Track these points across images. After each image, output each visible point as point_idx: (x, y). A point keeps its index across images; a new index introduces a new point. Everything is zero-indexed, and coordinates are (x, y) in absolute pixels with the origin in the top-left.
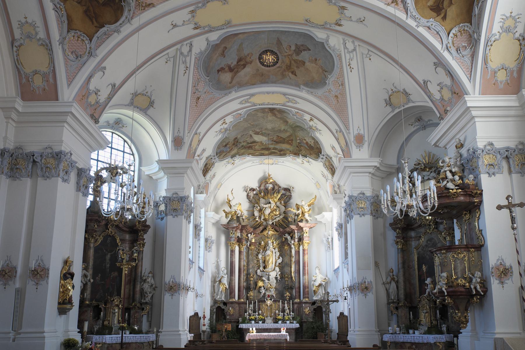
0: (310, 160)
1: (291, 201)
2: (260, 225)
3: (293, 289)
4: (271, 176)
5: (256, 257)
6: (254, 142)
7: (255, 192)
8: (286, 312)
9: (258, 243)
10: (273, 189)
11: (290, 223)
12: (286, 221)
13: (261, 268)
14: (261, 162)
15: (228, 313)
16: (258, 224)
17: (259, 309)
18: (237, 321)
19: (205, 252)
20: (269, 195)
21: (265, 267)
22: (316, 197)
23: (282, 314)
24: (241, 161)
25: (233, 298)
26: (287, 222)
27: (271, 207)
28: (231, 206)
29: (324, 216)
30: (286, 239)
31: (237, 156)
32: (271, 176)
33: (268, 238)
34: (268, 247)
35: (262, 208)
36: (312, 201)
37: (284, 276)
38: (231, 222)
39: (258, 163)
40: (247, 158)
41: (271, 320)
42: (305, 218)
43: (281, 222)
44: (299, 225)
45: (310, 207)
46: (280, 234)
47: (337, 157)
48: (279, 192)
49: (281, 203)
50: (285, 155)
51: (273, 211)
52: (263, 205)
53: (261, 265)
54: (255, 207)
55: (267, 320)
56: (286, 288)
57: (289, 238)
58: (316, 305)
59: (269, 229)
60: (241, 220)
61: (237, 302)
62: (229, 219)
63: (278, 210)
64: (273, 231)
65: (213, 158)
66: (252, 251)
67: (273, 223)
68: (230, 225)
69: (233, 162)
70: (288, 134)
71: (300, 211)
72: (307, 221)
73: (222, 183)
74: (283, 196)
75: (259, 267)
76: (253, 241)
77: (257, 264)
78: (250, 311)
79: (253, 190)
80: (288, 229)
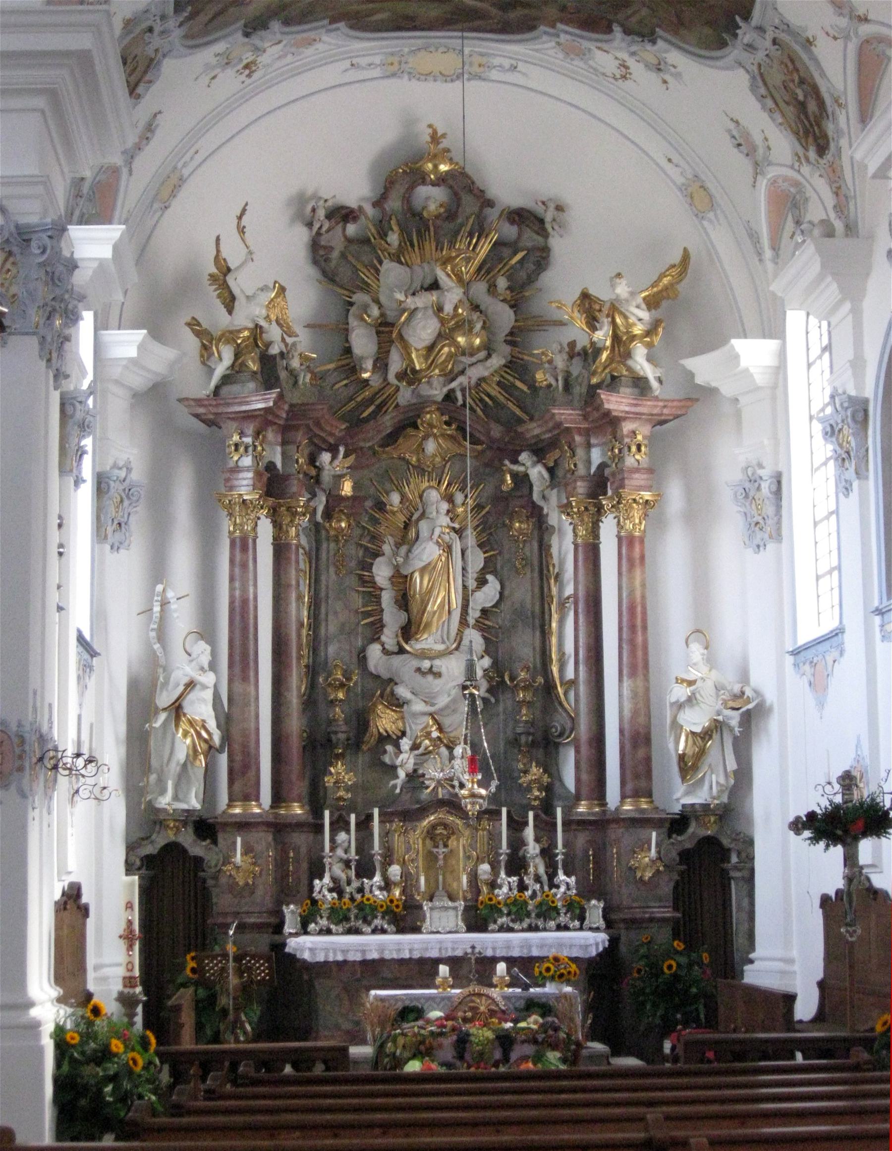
0: (674, 57)
1: (548, 278)
2: (380, 407)
3: (557, 745)
4: (445, 144)
5: (361, 577)
7: (351, 229)
8: (531, 870)
9: (368, 504)
10: (450, 214)
11: (541, 393)
12: (519, 384)
13: (389, 637)
14: (396, 67)
15: (223, 880)
16: (371, 401)
17: (388, 859)
18: (273, 920)
19: (96, 546)
20: (430, 246)
21: (408, 632)
22: (686, 257)
23: (514, 879)
24: (289, 58)
25: (246, 798)
26: (525, 388)
27: (440, 309)
28: (233, 298)
29: (737, 357)
30: (522, 480)
31: (275, 25)
32: (445, 144)
33: (421, 470)
34: (423, 525)
35: (391, 315)
36: (666, 281)
37: (512, 679)
38: (235, 389)
39: (377, 73)
40: (325, 38)
41: (451, 913)
42: (629, 369)
43: (494, 390)
44: (599, 407)
45: (657, 314)
46: (489, 454)
47: (847, 38)
48: (481, 230)
49: (492, 289)
50: (532, 28)
51: (452, 330)
52: (400, 296)
53: (387, 617)
54: (353, 310)
55: (436, 914)
56: (523, 739)
57: (537, 473)
58: (691, 830)
59: (431, 426)
60: (283, 375)
61: (271, 819)
62: (220, 370)
63: (479, 326)
64: (451, 437)
65: (157, 29)
66: (337, 541)
67: (449, 397)
68: (228, 405)
69: (248, 57)
71: (603, 335)
72: (640, 384)
73: (186, 172)
74: (506, 252)
75: (376, 630)
76: (347, 488)
77: (367, 614)
78: (338, 870)
80: (534, 430)
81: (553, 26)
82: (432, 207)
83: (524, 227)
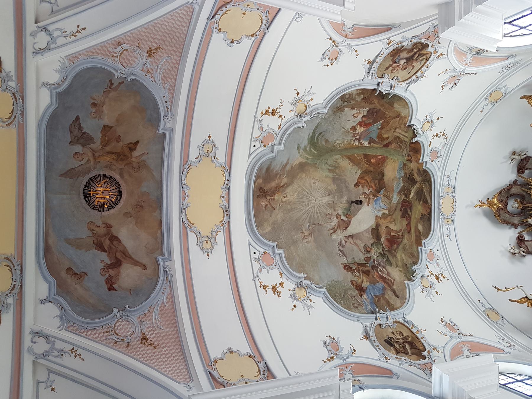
6: (375, 232)
7: (527, 238)
70: (345, 164)
73: (488, 306)
79: (520, 240)
81: (422, 164)
82: (516, 205)
83: (526, 167)
